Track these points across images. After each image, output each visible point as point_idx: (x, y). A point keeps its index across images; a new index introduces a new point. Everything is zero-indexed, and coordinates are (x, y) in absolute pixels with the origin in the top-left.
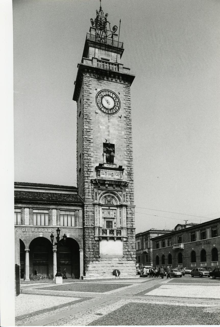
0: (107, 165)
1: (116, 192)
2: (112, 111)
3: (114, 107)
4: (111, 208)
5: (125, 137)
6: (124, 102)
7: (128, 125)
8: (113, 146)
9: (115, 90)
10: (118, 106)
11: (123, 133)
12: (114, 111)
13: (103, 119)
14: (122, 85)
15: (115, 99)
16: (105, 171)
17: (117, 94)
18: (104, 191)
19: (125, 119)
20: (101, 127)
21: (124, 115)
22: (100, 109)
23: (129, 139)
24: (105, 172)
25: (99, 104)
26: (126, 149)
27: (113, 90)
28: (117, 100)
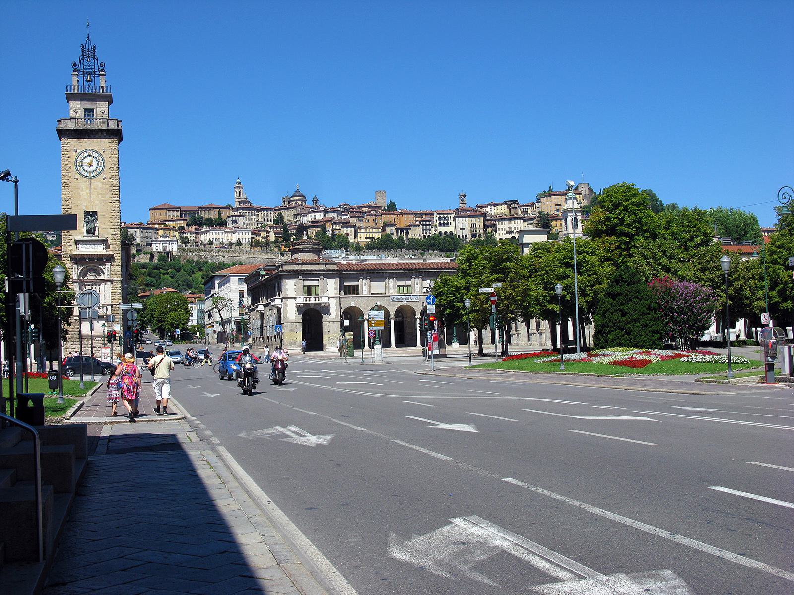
2: (94, 173)
3: (97, 168)
6: (110, 160)
8: (95, 213)
11: (108, 197)
12: (98, 173)
13: (83, 184)
15: (98, 158)
17: (101, 152)
19: (110, 180)
20: (81, 194)
22: (81, 174)
25: (79, 168)
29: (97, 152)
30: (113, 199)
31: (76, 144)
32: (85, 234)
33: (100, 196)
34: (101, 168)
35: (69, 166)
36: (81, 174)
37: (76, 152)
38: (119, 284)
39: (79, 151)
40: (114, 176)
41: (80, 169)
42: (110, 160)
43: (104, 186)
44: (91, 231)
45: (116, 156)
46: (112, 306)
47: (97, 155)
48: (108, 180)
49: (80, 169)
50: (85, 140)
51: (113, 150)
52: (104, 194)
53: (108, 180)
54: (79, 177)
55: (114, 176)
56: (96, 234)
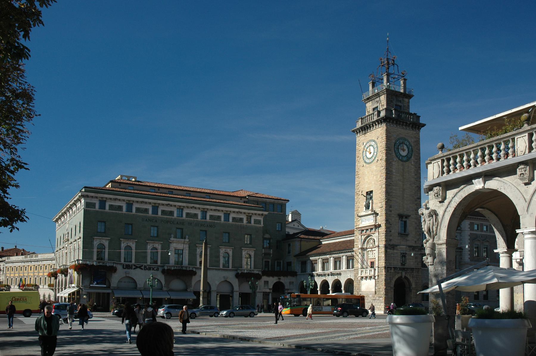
1: (372, 235)
4: (373, 249)
5: (380, 180)
7: (382, 167)
8: (371, 192)
11: (379, 177)
12: (374, 158)
14: (379, 129)
17: (376, 140)
18: (366, 236)
21: (380, 158)
22: (365, 162)
23: (382, 180)
26: (380, 191)
29: (374, 141)
32: (364, 210)
33: (375, 177)
34: (376, 153)
36: (365, 162)
38: (383, 250)
42: (381, 144)
44: (367, 207)
45: (384, 140)
46: (378, 267)
47: (374, 143)
48: (380, 161)
50: (368, 133)
52: (377, 175)
53: (380, 161)
54: (365, 164)
56: (370, 208)
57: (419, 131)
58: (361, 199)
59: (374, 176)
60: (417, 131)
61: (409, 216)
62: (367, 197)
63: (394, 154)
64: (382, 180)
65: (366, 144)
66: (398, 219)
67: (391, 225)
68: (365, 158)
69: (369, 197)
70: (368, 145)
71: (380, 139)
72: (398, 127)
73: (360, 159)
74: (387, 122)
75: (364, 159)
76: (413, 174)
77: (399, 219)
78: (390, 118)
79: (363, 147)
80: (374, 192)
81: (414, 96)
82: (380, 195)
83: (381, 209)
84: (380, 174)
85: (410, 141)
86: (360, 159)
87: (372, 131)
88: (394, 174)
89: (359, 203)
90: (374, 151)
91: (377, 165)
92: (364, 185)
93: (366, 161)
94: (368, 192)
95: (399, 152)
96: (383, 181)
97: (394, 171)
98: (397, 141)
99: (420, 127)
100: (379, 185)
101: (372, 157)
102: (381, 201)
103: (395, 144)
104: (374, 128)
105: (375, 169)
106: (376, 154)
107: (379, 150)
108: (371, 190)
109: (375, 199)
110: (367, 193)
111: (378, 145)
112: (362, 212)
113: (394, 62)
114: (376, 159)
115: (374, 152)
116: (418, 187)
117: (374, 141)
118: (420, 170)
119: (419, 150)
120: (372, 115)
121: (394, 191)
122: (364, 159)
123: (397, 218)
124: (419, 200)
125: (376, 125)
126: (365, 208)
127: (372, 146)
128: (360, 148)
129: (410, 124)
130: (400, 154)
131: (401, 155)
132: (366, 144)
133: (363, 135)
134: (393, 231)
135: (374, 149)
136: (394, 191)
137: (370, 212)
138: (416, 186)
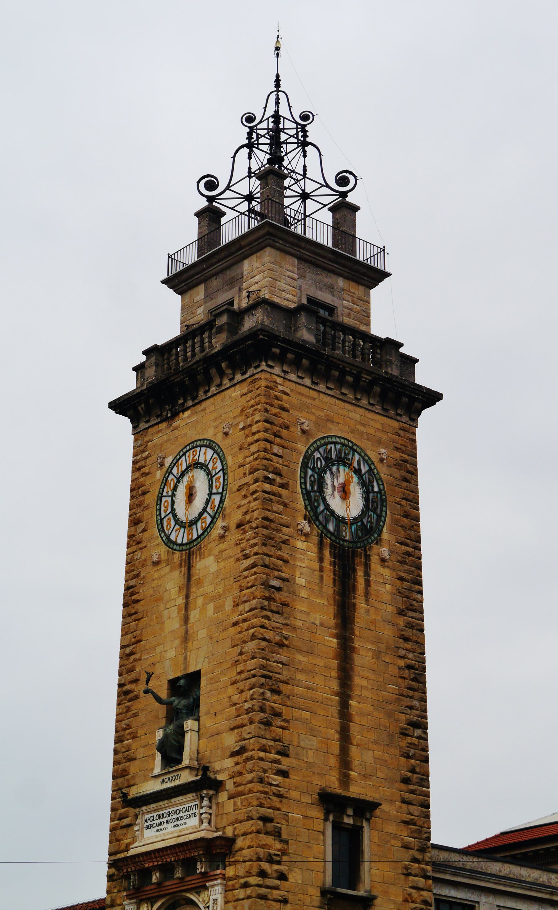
0: (163, 782)
2: (199, 524)
3: (207, 502)
5: (235, 618)
7: (246, 557)
9: (216, 427)
10: (220, 490)
11: (229, 604)
12: (209, 520)
16: (156, 810)
17: (219, 439)
21: (237, 517)
23: (245, 620)
24: (155, 814)
26: (233, 674)
27: (209, 435)
28: (219, 466)
29: (211, 444)
30: (241, 608)
31: (165, 438)
32: (157, 770)
34: (217, 499)
35: (142, 526)
37: (162, 465)
39: (168, 461)
40: (248, 517)
41: (169, 523)
42: (240, 459)
43: (222, 564)
47: (210, 452)
48: (234, 536)
49: (169, 523)
50: (187, 414)
51: (249, 421)
52: (220, 596)
55: (248, 517)
57: (415, 420)
58: (142, 717)
59: (205, 604)
60: (405, 419)
61: (373, 806)
62: (169, 704)
63: (300, 503)
64: (245, 620)
65: (176, 462)
66: (322, 816)
67: (286, 842)
68: (169, 524)
69: (180, 703)
70: (184, 463)
71: (238, 436)
72: (322, 387)
73: (144, 530)
74: (274, 357)
75: (161, 530)
76: (389, 608)
77: (326, 819)
78: (284, 340)
79: (159, 475)
80: (203, 682)
81: (388, 275)
82: (231, 690)
83: (236, 759)
84: (236, 593)
85: (372, 455)
86: (144, 530)
87: (204, 404)
88: (303, 593)
89: (134, 736)
90: (211, 487)
91: (221, 552)
92: (159, 649)
93: (173, 537)
94: (178, 679)
95: (324, 500)
96: (246, 625)
97: (302, 581)
98: (317, 449)
99: (417, 405)
100: (229, 643)
101: (201, 515)
102: (239, 721)
103: (307, 458)
104: (213, 389)
105: (213, 568)
106: (217, 503)
107: (233, 485)
108: (192, 669)
109: (207, 713)
110: (173, 683)
111: (230, 460)
112: (145, 780)
113: (305, 136)
114: (220, 523)
115: (210, 494)
116: (409, 667)
117: (211, 444)
118: (421, 592)
119: (414, 502)
120: (206, 335)
121: (300, 676)
122: (161, 530)
123: (317, 813)
124: (418, 732)
125: (222, 374)
126: (159, 756)
127: (203, 466)
128: (148, 481)
129: (371, 384)
130: (327, 507)
131: (332, 512)
132: (176, 462)
133: (164, 425)
134: (295, 877)
135: (211, 480)
136: (300, 676)
137: (186, 777)
138: (402, 663)
